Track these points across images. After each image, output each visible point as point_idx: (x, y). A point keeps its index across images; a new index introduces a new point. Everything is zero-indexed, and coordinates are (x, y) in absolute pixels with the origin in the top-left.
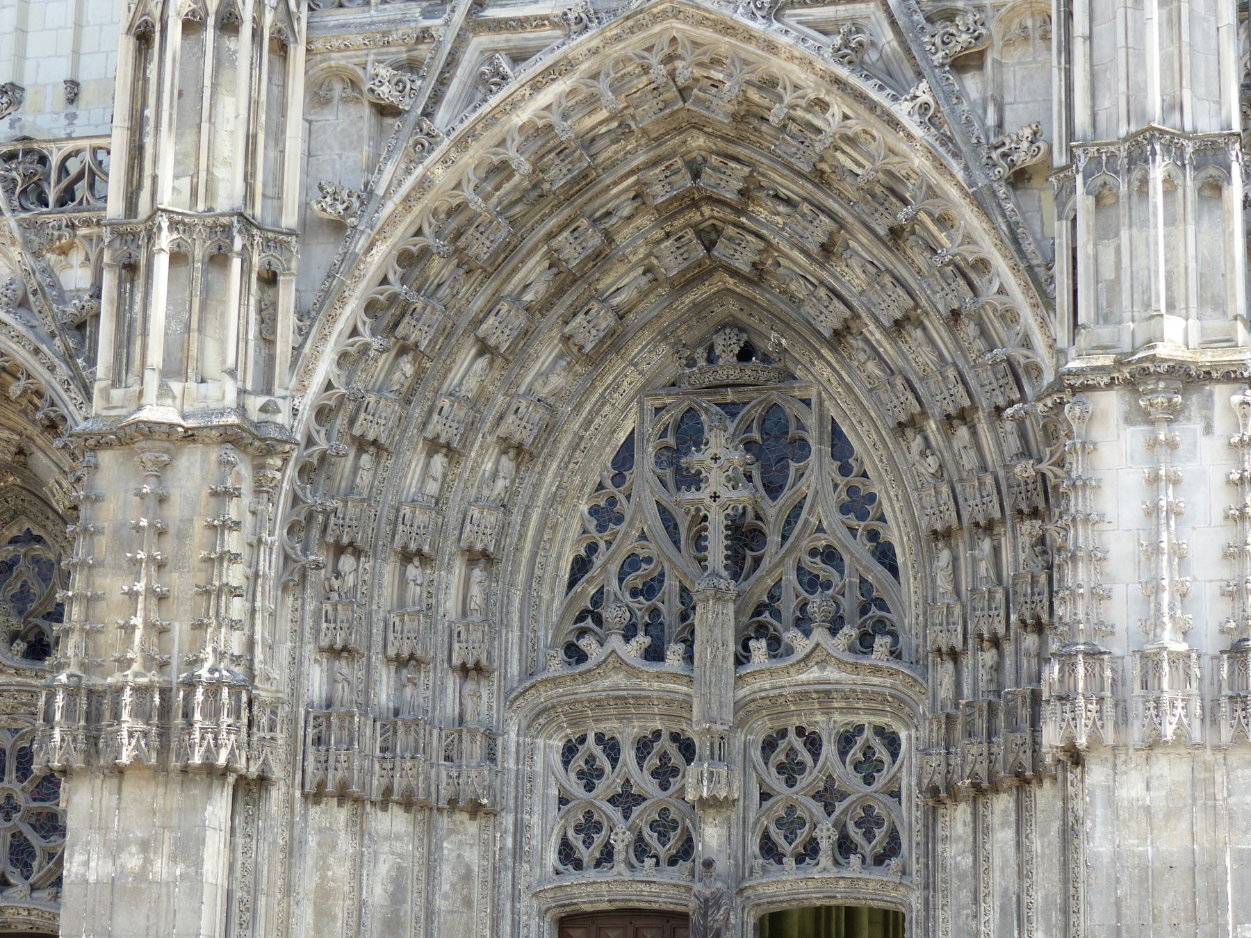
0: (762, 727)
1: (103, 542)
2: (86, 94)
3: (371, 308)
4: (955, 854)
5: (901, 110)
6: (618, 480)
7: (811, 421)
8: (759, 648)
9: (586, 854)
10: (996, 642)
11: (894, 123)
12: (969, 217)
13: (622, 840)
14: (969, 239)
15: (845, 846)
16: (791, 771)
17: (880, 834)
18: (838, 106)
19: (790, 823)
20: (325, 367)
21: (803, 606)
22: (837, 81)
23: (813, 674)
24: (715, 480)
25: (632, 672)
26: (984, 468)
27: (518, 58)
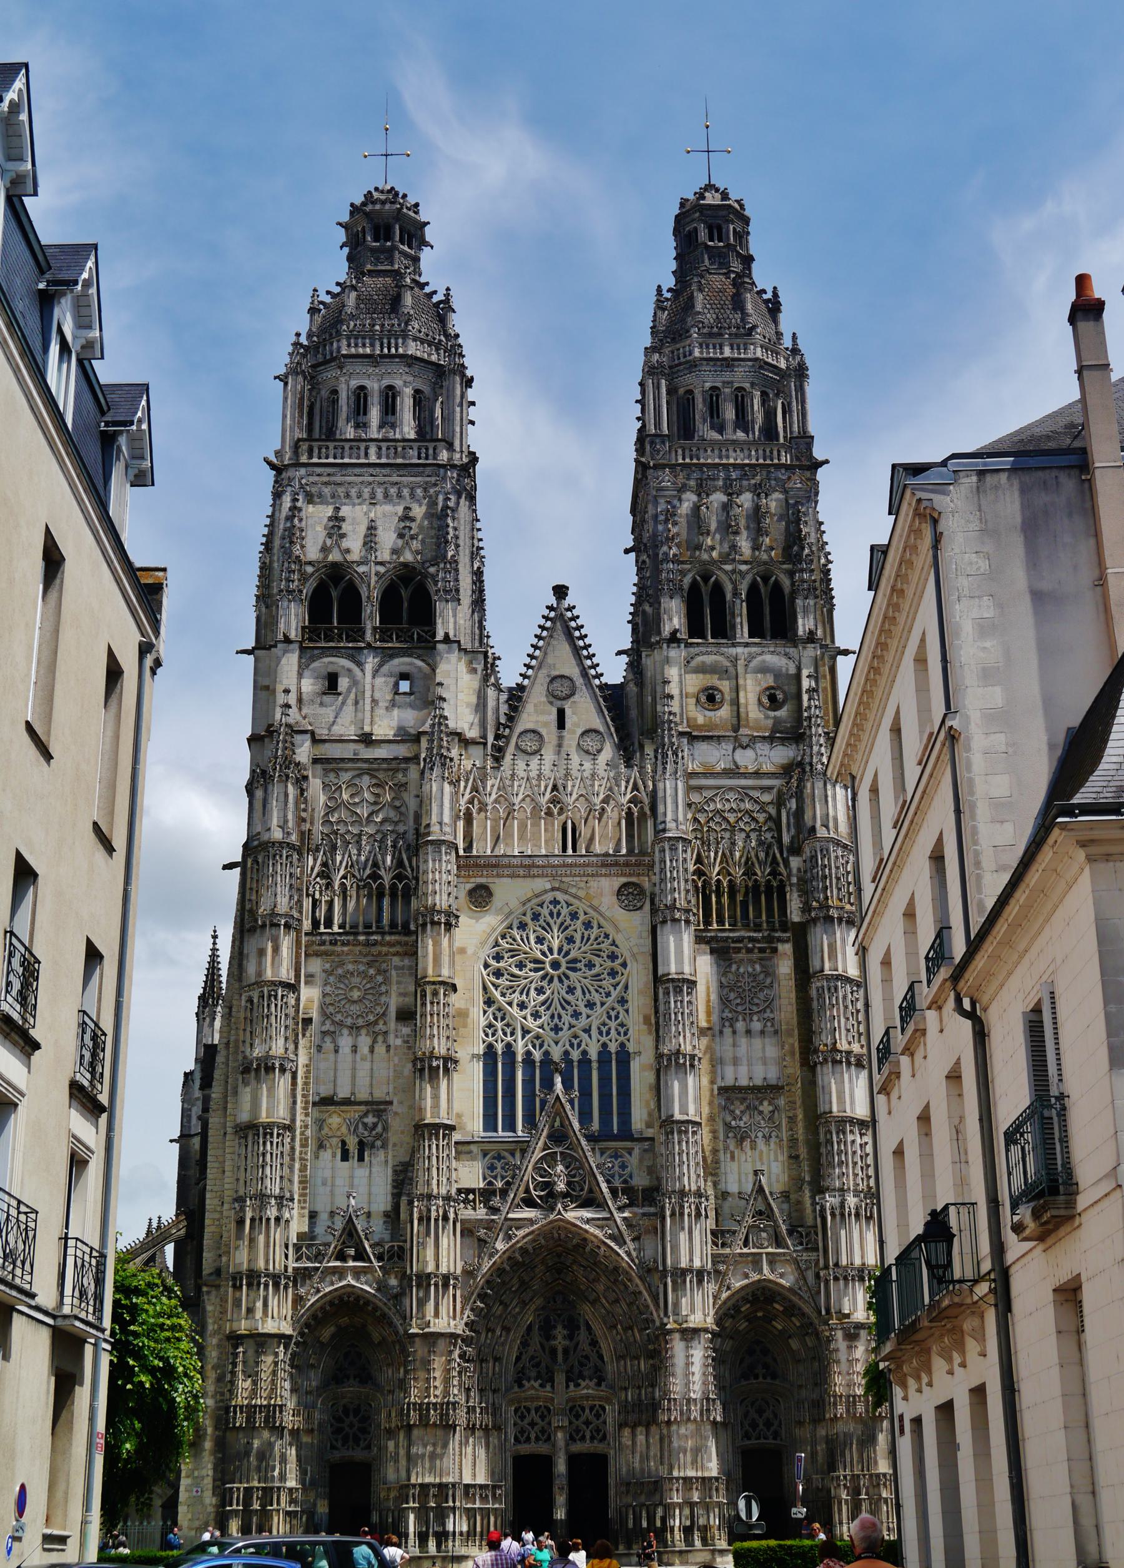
0: (570, 1404)
1: (418, 1363)
2: (373, 1215)
3: (479, 1295)
4: (626, 1440)
5: (621, 1252)
6: (528, 1334)
7: (581, 1320)
8: (572, 1385)
9: (522, 1440)
10: (639, 1388)
11: (619, 1255)
12: (638, 1281)
13: (533, 1436)
14: (637, 1285)
15: (592, 1438)
16: (577, 1417)
17: (601, 1434)
18: (603, 1248)
19: (578, 1431)
20: (467, 1312)
21: (580, 1372)
22: (605, 1244)
23: (585, 1391)
24: (560, 1337)
25: (536, 1390)
26: (635, 1341)
27: (517, 1228)
